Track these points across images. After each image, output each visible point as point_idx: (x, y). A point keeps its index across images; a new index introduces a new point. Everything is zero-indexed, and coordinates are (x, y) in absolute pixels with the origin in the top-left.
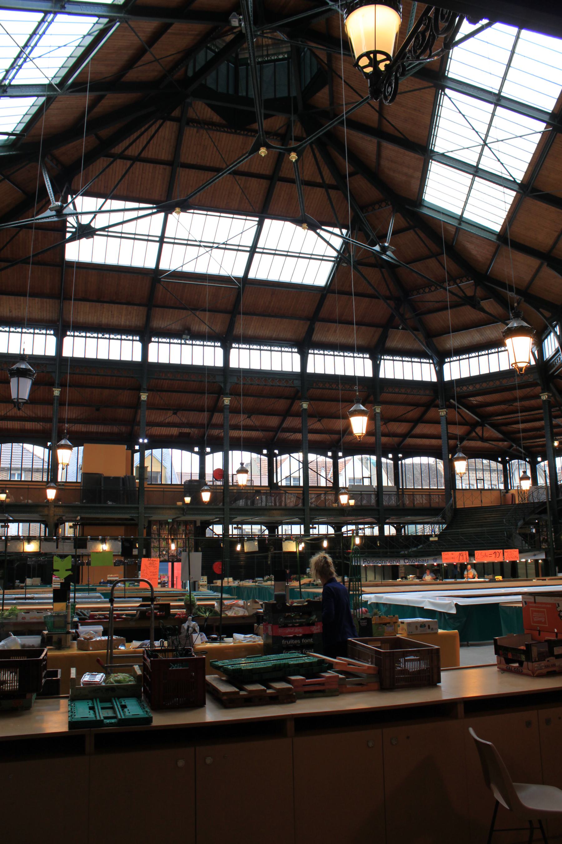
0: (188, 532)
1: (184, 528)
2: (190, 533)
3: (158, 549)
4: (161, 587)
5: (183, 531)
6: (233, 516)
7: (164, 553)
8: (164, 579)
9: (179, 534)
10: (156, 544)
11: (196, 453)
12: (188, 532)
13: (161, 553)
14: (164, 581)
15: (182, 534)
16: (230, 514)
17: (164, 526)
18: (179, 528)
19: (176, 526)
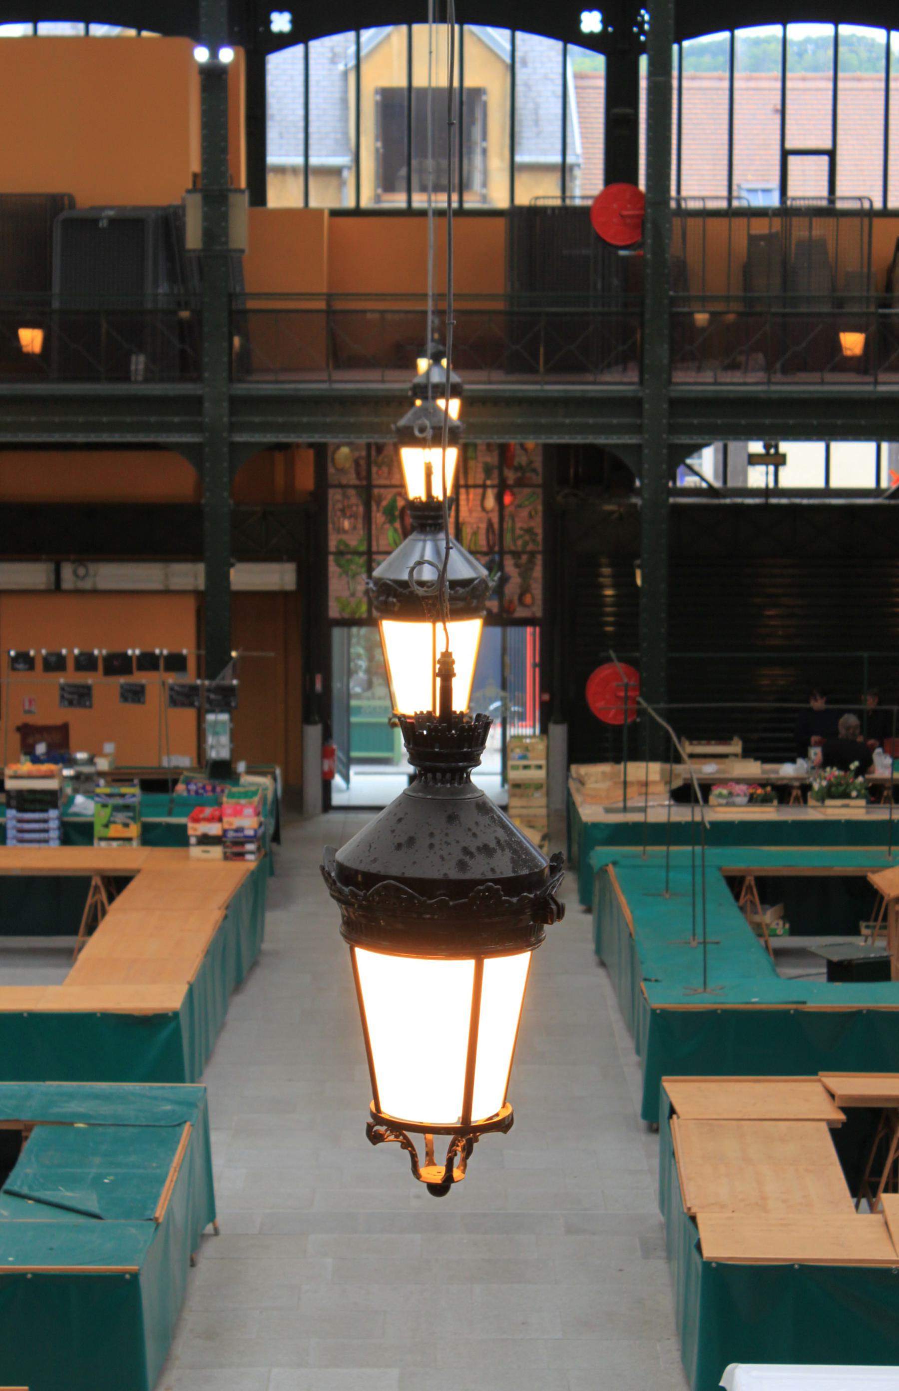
0: (511, 476)
2: (521, 483)
3: (362, 560)
4: (226, 857)
5: (488, 471)
6: (685, 440)
8: (237, 822)
10: (355, 541)
11: (590, 42)
12: (511, 476)
14: (239, 830)
15: (484, 487)
16: (674, 429)
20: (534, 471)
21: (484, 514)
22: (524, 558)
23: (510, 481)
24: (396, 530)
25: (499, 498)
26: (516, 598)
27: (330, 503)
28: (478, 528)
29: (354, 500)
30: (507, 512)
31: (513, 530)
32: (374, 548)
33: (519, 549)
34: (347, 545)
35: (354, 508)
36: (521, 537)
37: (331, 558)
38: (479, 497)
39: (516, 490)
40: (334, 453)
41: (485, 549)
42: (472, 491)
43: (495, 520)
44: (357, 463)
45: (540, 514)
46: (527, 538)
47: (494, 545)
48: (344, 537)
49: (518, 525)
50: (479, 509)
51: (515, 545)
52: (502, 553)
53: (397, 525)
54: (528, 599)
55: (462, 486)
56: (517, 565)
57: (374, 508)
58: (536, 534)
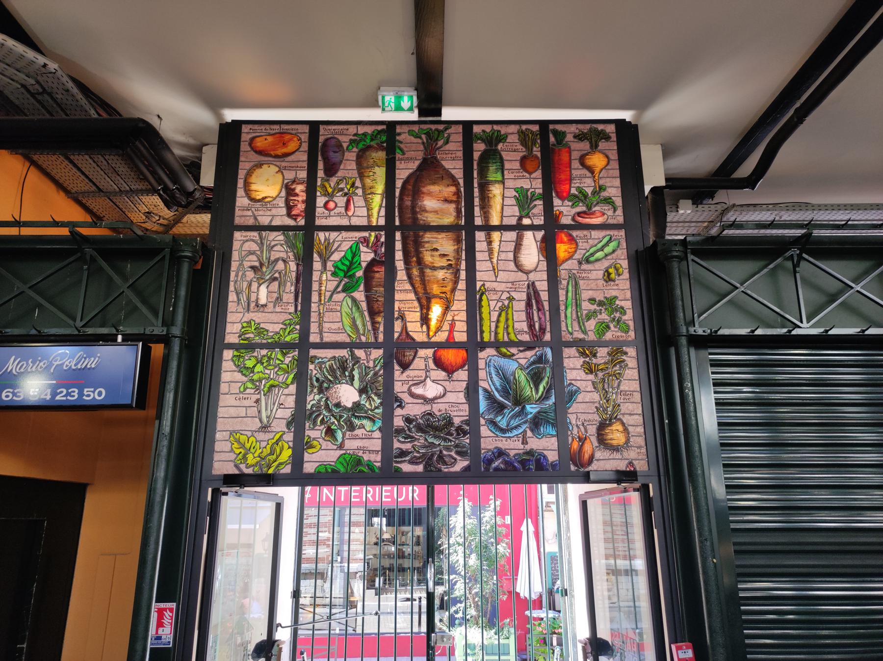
0: (566, 211)
1: (534, 183)
5: (524, 201)
7: (347, 394)
9: (488, 228)
13: (313, 399)
17: (348, 167)
18: (484, 187)
19: (456, 167)
20: (608, 201)
21: (521, 276)
22: (602, 352)
23: (566, 220)
24: (354, 300)
25: (548, 248)
26: (592, 430)
27: (235, 256)
28: (511, 299)
29: (280, 252)
30: (563, 271)
31: (577, 305)
32: (314, 338)
33: (592, 337)
34: (260, 331)
35: (280, 266)
36: (591, 315)
37: (228, 354)
38: (512, 246)
39: (575, 233)
40: (249, 174)
41: (526, 338)
42: (496, 235)
43: (542, 286)
44: (290, 192)
45: (626, 275)
46: (604, 316)
47: (543, 330)
48: (257, 317)
49: (585, 295)
50: (512, 266)
51: (585, 332)
52: (558, 345)
53: (360, 295)
54: (616, 435)
55: (480, 228)
56: (590, 369)
57: (317, 265)
58: (623, 311)
